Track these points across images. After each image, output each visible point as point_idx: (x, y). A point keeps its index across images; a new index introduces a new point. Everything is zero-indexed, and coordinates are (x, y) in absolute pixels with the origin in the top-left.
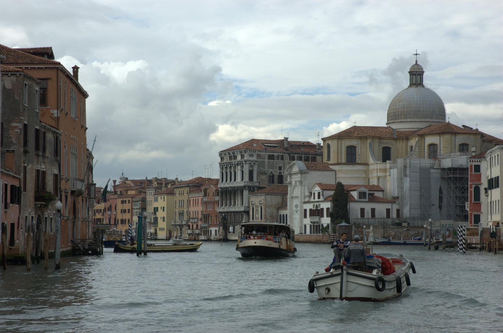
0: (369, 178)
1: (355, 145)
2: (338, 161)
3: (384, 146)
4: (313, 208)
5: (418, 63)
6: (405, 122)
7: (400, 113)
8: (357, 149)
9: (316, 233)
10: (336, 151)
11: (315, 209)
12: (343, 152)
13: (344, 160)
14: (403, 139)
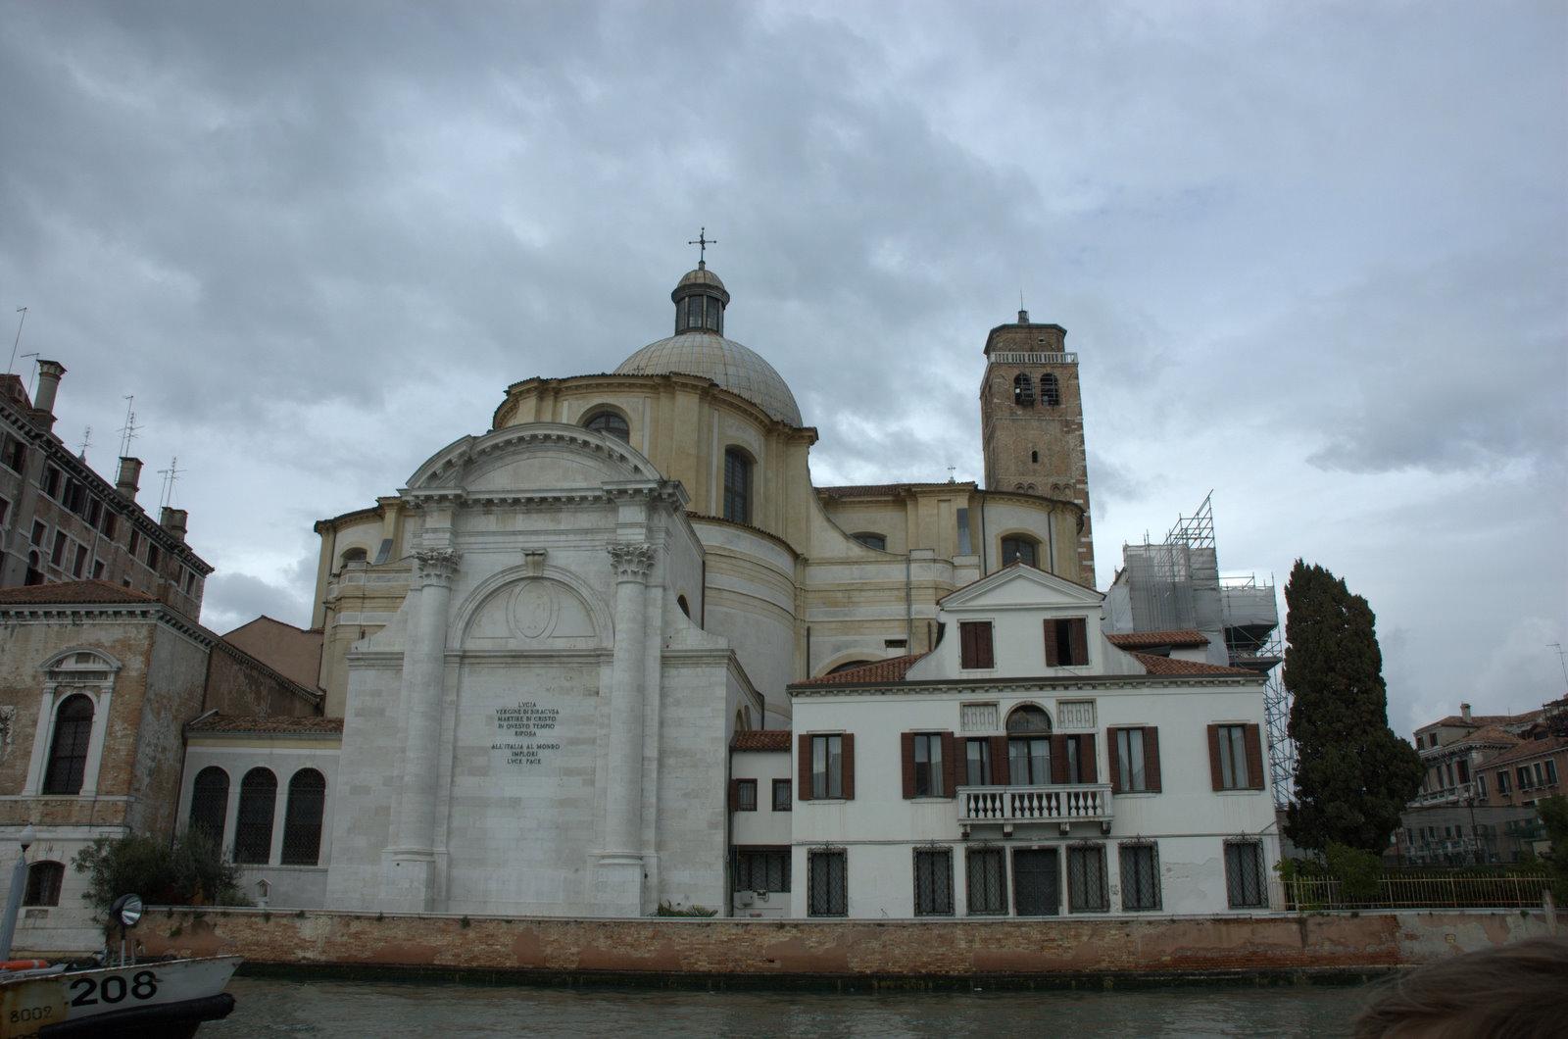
0: (808, 629)
4: (963, 724)
5: (707, 267)
12: (714, 468)
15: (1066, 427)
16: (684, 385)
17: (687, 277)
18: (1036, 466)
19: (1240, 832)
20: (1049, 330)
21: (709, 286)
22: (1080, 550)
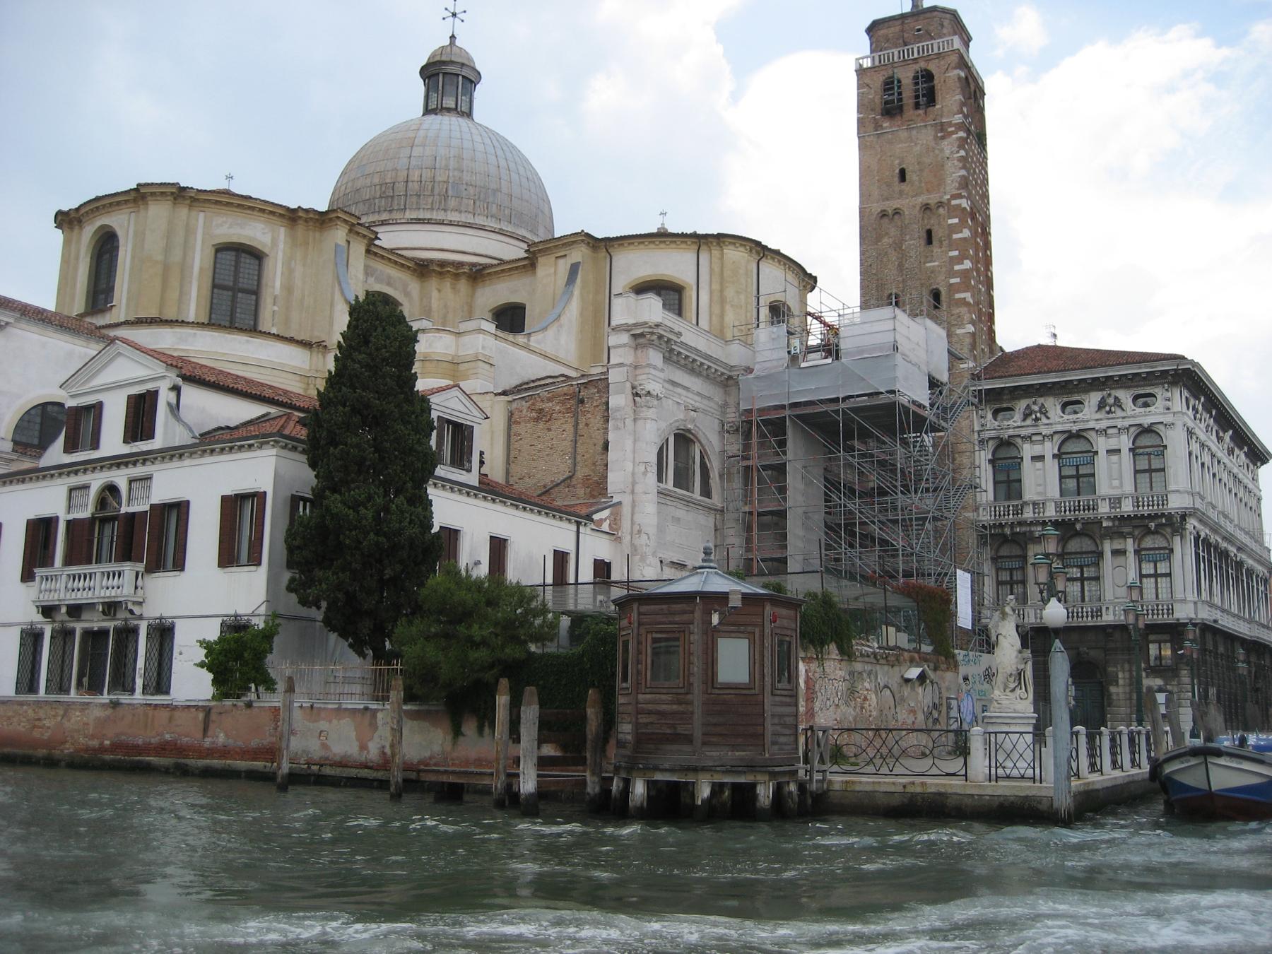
1: (260, 247)
2: (161, 307)
3: (378, 287)
5: (458, 43)
6: (441, 223)
7: (413, 187)
8: (269, 265)
9: (79, 684)
10: (160, 258)
11: (85, 512)
13: (193, 311)
14: (457, 276)
15: (942, 130)
16: (153, 194)
17: (433, 55)
18: (904, 186)
19: (233, 613)
20: (928, 15)
21: (444, 63)
22: (952, 281)
